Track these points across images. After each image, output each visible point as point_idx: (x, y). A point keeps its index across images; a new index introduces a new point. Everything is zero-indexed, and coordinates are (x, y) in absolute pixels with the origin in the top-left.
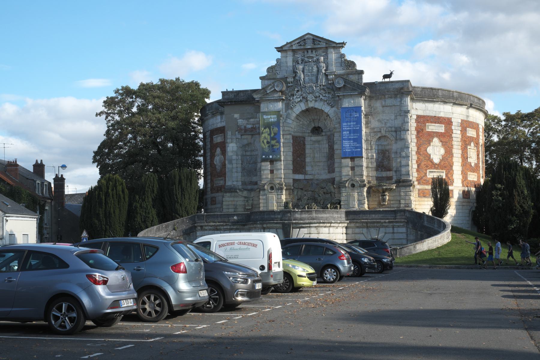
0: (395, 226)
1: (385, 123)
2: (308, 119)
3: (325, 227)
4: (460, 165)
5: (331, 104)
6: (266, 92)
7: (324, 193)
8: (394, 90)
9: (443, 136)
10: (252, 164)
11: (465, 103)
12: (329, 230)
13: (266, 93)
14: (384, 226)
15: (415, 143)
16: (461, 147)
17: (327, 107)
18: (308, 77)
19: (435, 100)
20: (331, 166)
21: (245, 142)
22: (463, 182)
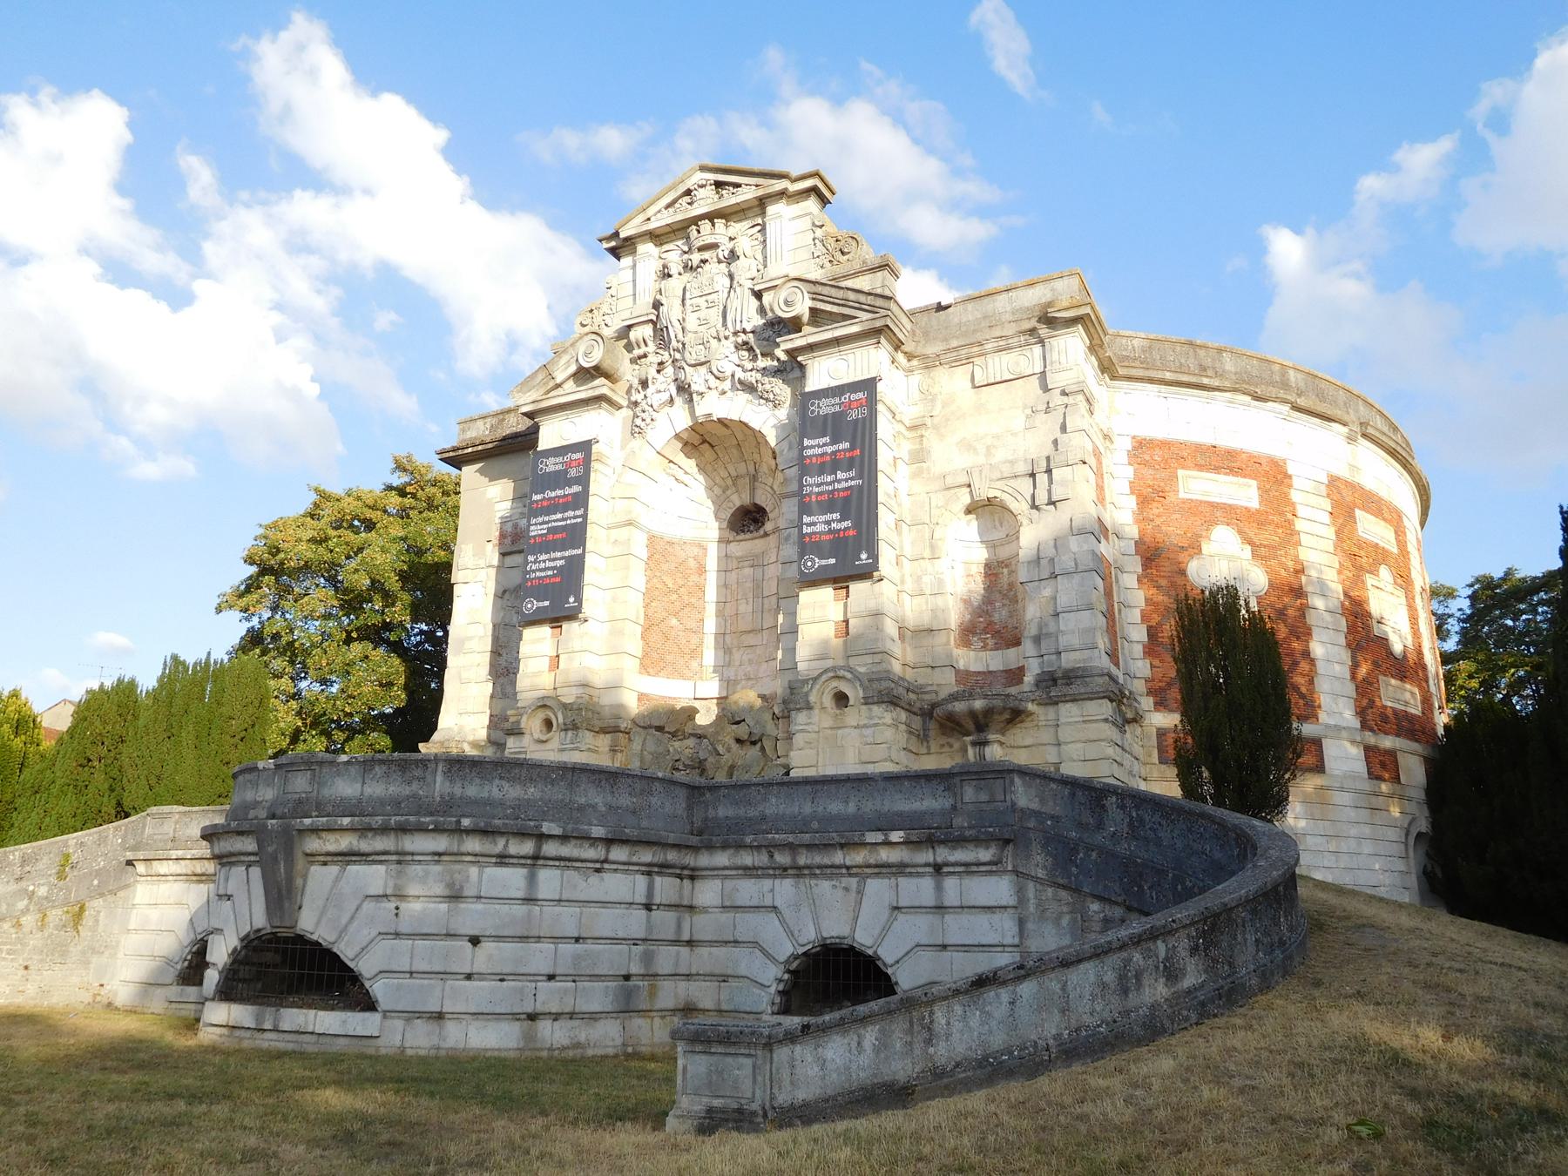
0: (947, 864)
1: (988, 448)
2: (718, 480)
3: (503, 859)
4: (1342, 641)
7: (738, 741)
8: (1016, 317)
9: (1255, 525)
11: (1337, 413)
12: (532, 880)
13: (551, 384)
14: (889, 866)
15: (1133, 542)
16: (1339, 572)
19: (1205, 381)
22: (1361, 713)
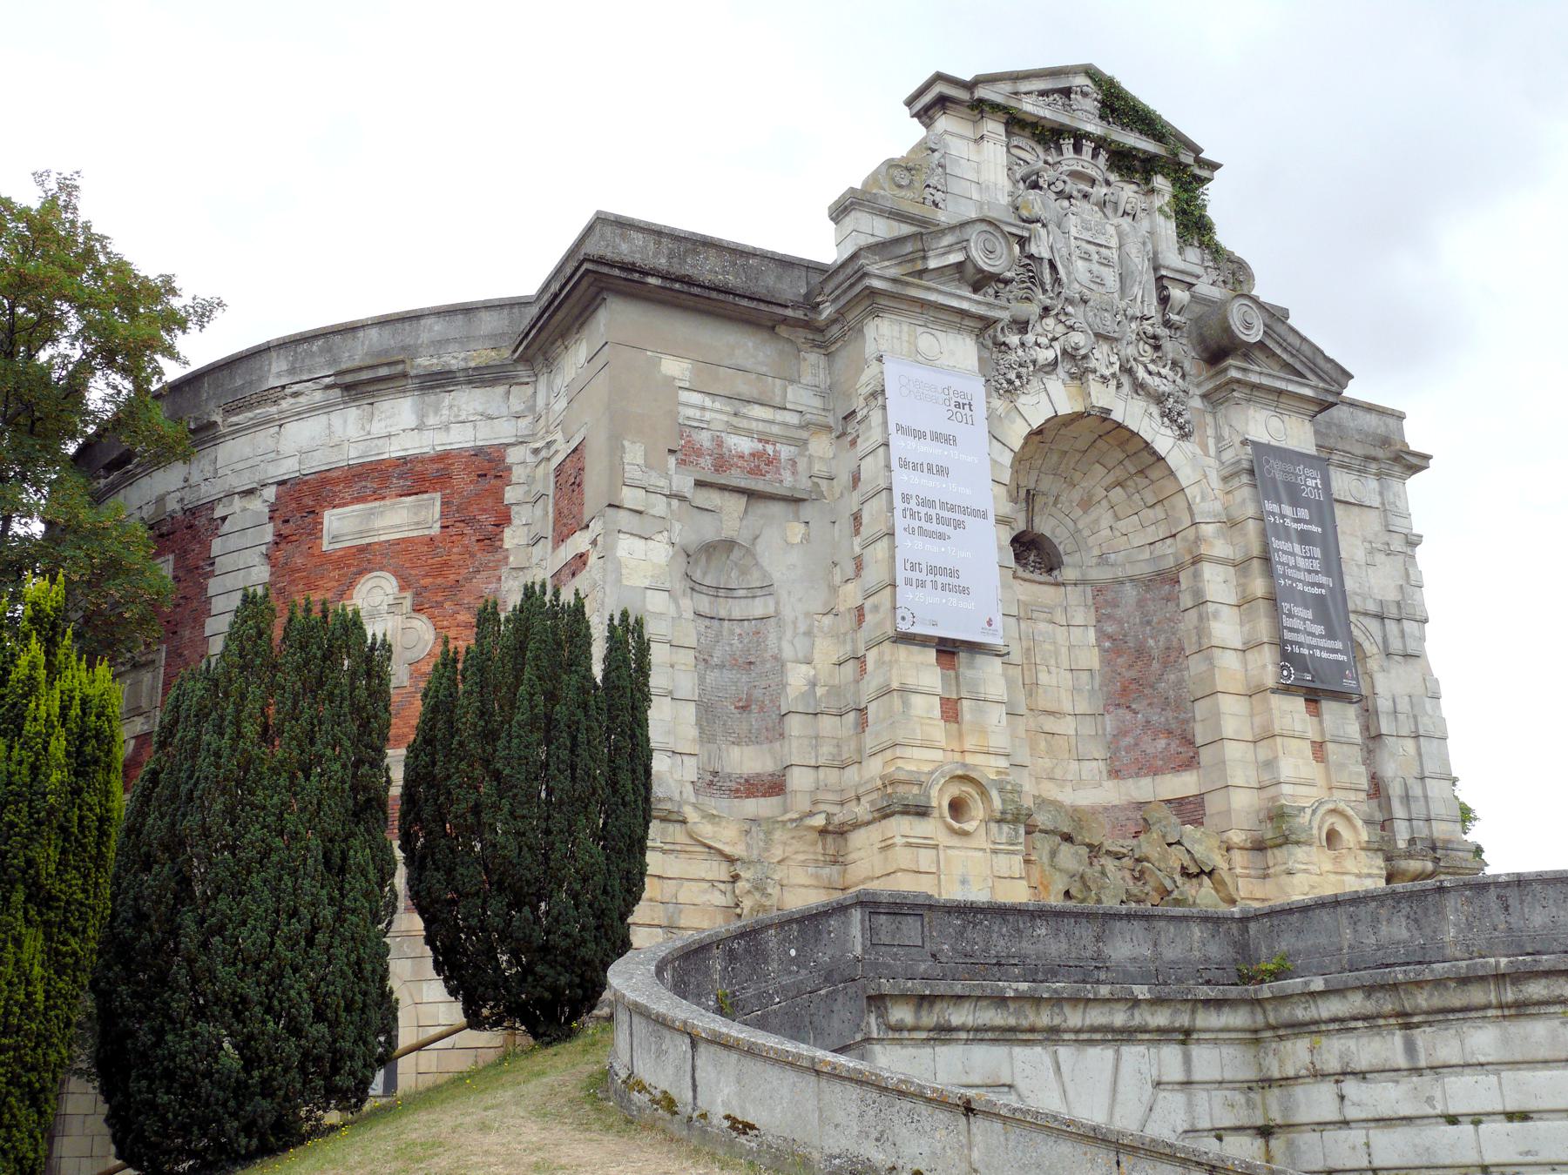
5: (1181, 420)
6: (925, 258)
10: (722, 666)
13: (919, 266)
17: (1163, 430)
18: (1086, 264)
20: (1129, 740)
21: (708, 530)
